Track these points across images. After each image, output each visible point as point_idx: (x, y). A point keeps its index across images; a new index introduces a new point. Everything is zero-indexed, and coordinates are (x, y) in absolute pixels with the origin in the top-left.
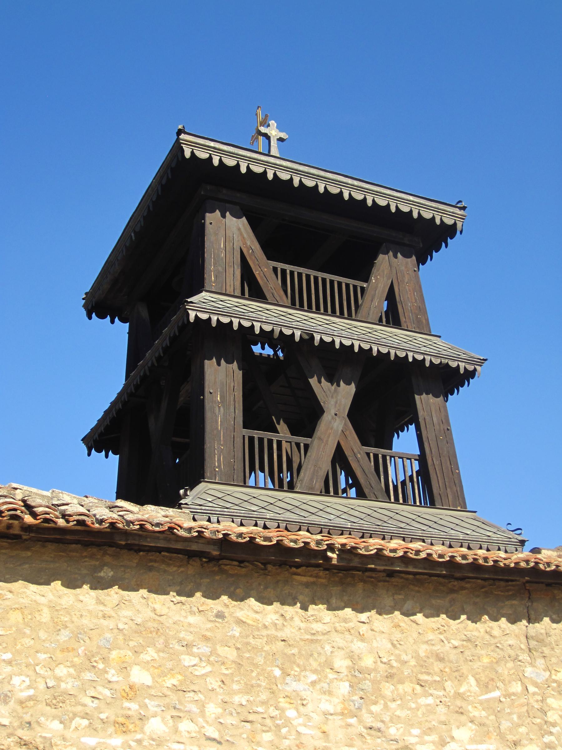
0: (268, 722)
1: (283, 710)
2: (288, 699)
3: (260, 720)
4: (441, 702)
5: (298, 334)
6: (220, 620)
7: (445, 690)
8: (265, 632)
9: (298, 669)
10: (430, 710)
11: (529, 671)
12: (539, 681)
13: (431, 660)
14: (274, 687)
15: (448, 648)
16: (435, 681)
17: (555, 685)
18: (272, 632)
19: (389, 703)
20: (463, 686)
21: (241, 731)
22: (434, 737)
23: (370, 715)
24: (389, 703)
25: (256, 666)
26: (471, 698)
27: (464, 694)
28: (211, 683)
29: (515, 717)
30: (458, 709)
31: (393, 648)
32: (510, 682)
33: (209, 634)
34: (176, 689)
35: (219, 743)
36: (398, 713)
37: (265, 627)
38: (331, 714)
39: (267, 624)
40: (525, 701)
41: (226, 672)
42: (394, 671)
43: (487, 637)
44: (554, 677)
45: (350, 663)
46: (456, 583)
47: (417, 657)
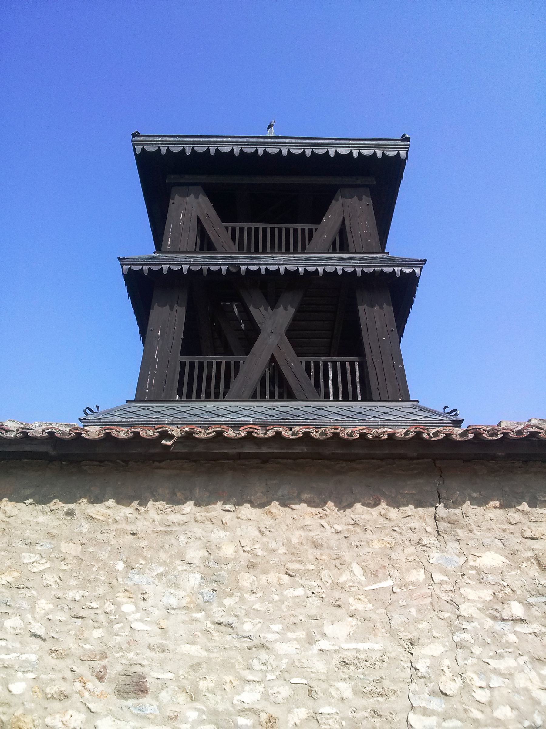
0: (102, 618)
1: (119, 605)
2: (127, 594)
3: (93, 616)
4: (313, 593)
5: (224, 268)
6: (69, 518)
7: (321, 580)
8: (114, 527)
9: (143, 562)
10: (298, 602)
11: (435, 557)
12: (449, 568)
13: (305, 547)
14: (114, 581)
15: (329, 533)
16: (308, 570)
17: (474, 572)
18: (124, 526)
19: (246, 596)
20: (344, 575)
21: (70, 627)
22: (301, 634)
23: (221, 610)
24: (246, 596)
25: (99, 560)
26: (353, 589)
27: (344, 583)
28: (46, 580)
29: (413, 611)
30: (334, 602)
31: (260, 536)
32: (408, 570)
33: (54, 531)
34: (10, 586)
35: (44, 640)
36: (257, 606)
37: (116, 521)
38: (174, 609)
39: (117, 518)
40: (429, 591)
41: (65, 568)
42: (259, 560)
43: (382, 520)
44: (471, 563)
45: (206, 553)
46: (344, 465)
47: (288, 543)
